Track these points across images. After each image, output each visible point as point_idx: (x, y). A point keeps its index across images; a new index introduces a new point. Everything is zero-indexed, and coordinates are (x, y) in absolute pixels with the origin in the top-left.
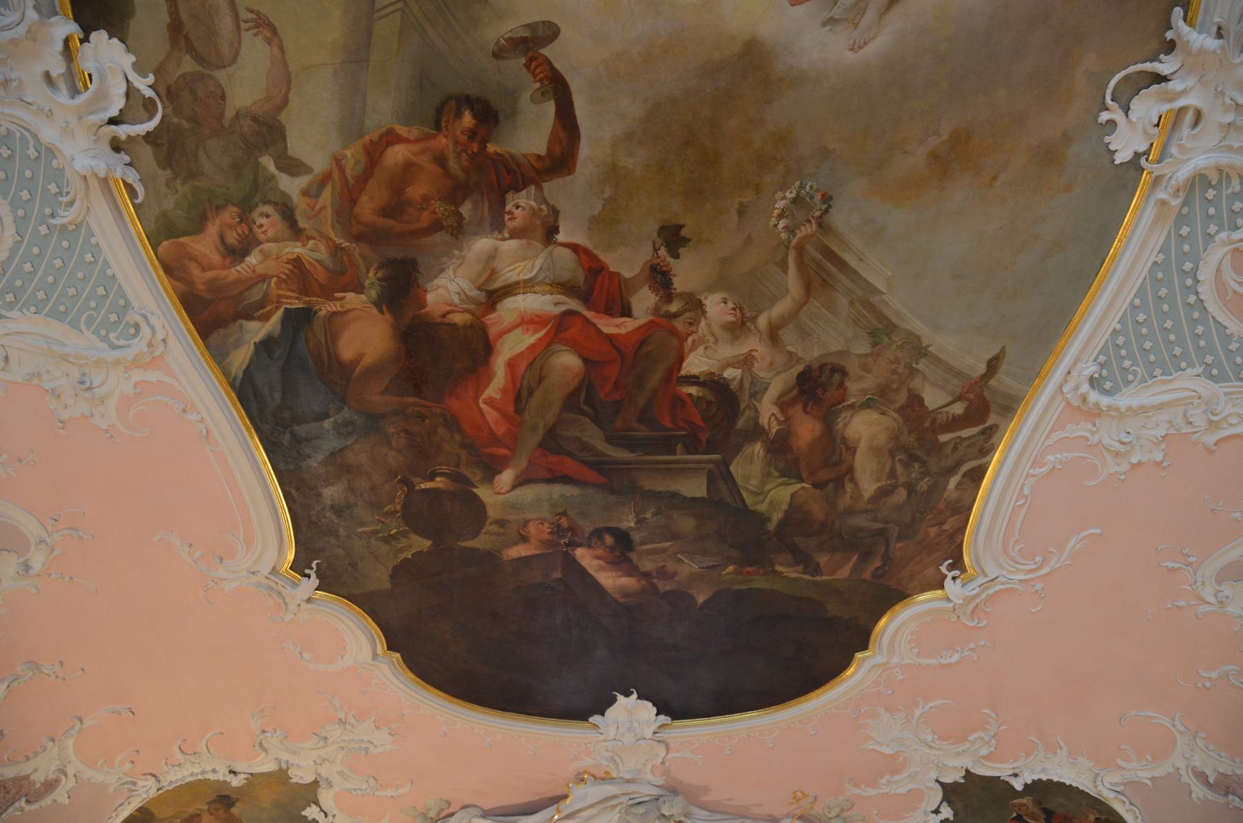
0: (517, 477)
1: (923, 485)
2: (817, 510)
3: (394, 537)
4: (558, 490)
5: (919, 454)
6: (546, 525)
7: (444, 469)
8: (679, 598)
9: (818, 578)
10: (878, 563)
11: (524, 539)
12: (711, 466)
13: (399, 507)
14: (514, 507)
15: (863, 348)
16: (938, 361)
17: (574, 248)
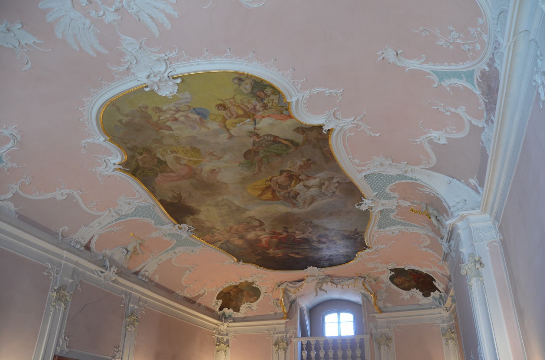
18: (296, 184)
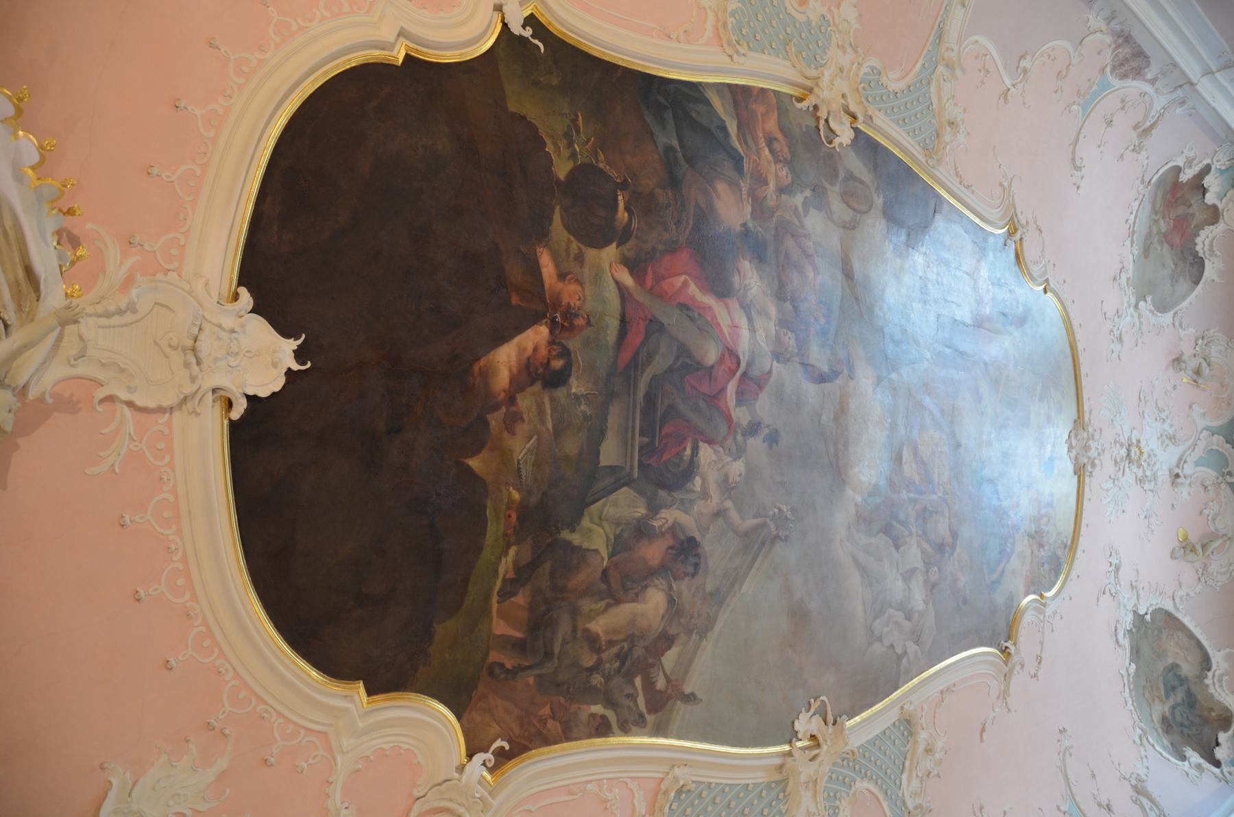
0: (626, 288)
1: (597, 680)
2: (580, 579)
3: (570, 144)
4: (613, 324)
5: (628, 663)
6: (578, 303)
7: (635, 225)
8: (477, 436)
9: (495, 598)
10: (508, 665)
11: (562, 276)
12: (628, 469)
13: (601, 165)
14: (597, 278)
15: (710, 587)
16: (697, 648)
17: (770, 372)
18: (923, 552)
